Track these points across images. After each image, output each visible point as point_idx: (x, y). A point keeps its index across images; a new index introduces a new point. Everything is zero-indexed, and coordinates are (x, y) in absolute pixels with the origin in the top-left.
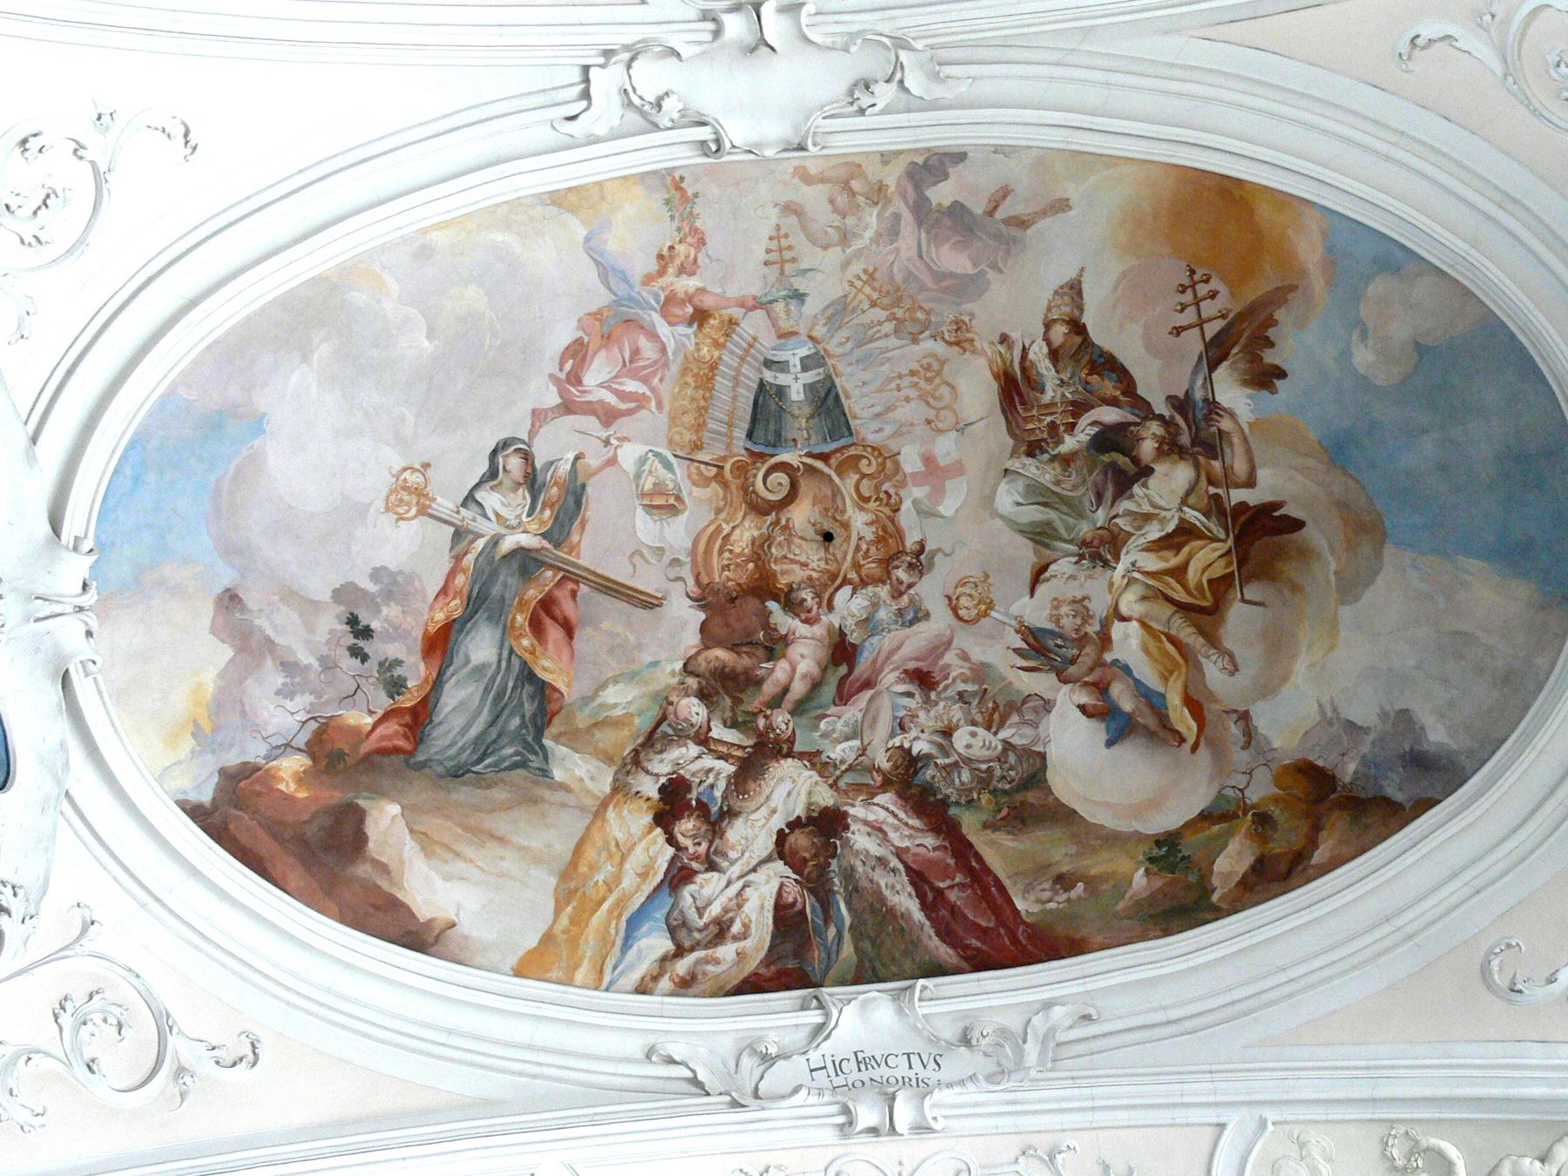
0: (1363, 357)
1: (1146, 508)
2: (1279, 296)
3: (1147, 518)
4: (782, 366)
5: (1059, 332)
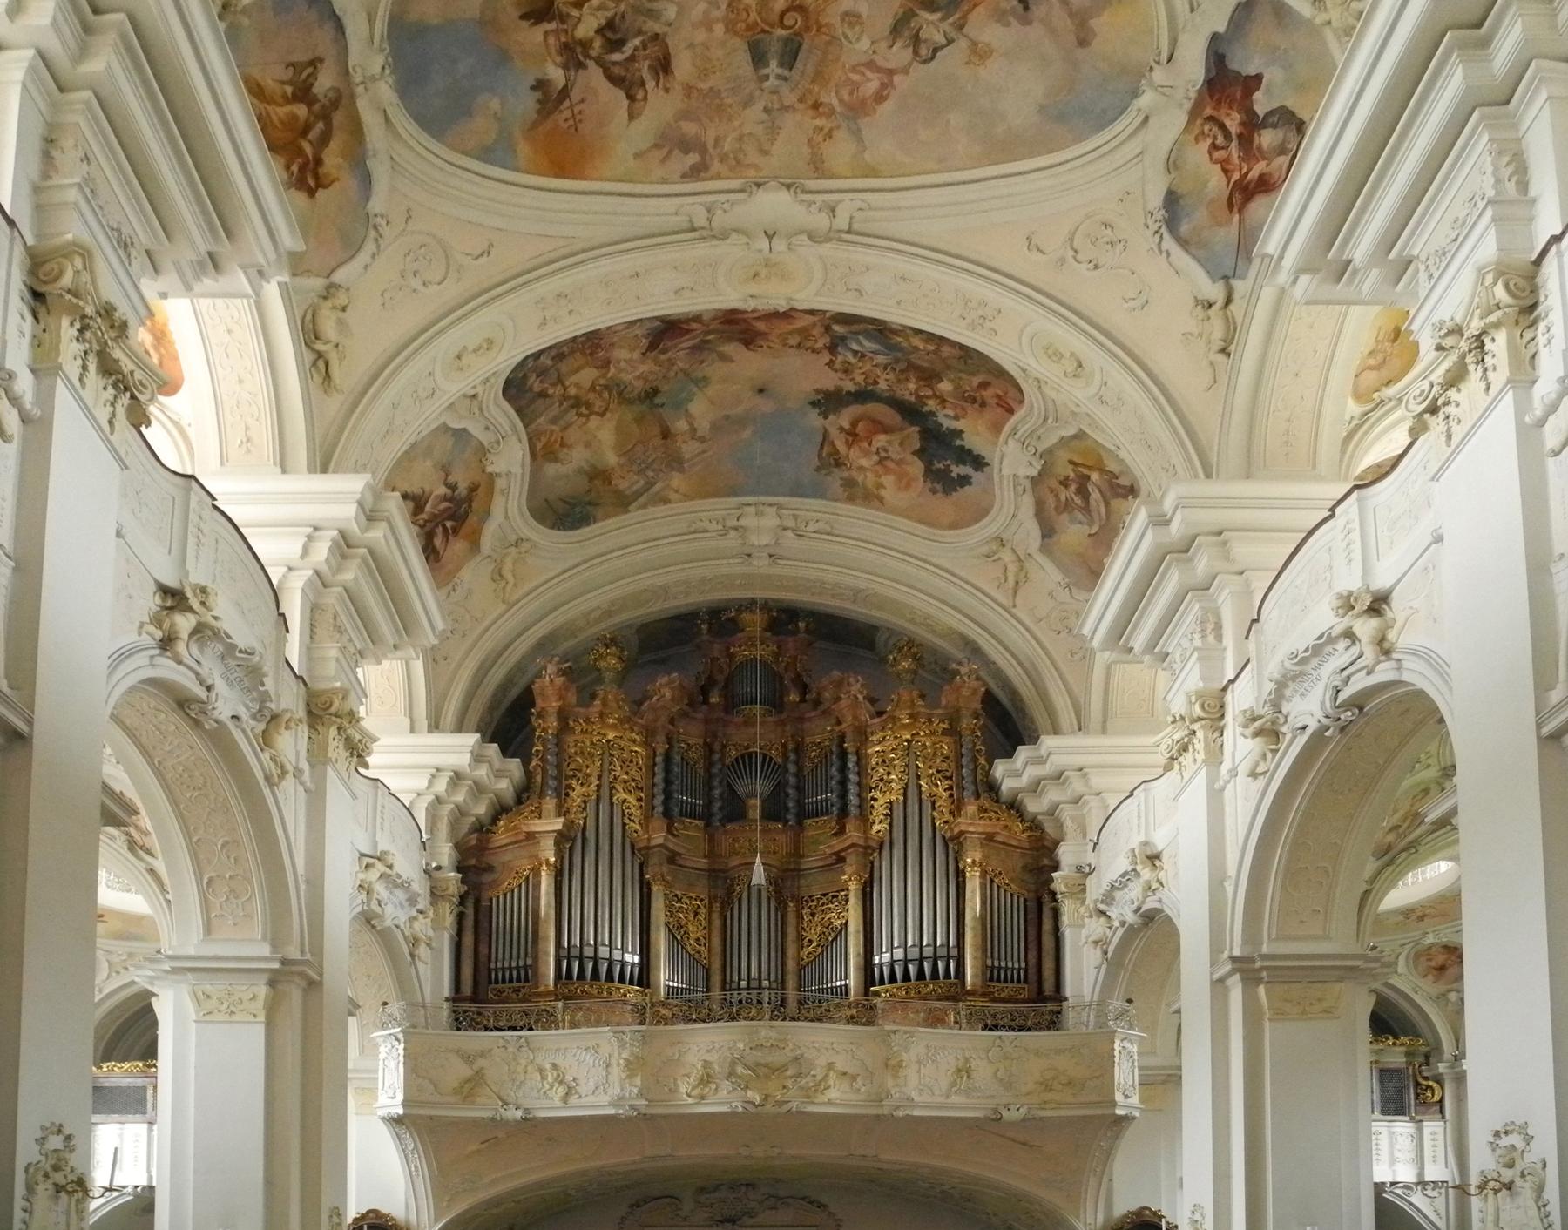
0: (495, 104)
1: (599, 14)
2: (534, 125)
3: (599, 9)
4: (779, 77)
5: (640, 95)
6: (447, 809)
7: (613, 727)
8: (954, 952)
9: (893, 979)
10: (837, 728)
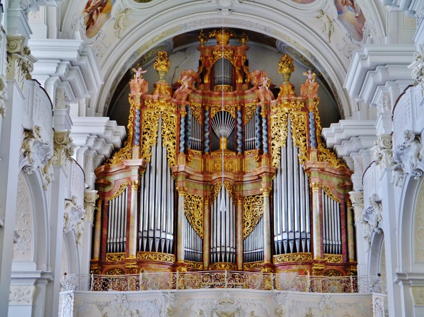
6: (93, 152)
7: (163, 104)
8: (309, 236)
9: (283, 252)
10: (258, 104)
